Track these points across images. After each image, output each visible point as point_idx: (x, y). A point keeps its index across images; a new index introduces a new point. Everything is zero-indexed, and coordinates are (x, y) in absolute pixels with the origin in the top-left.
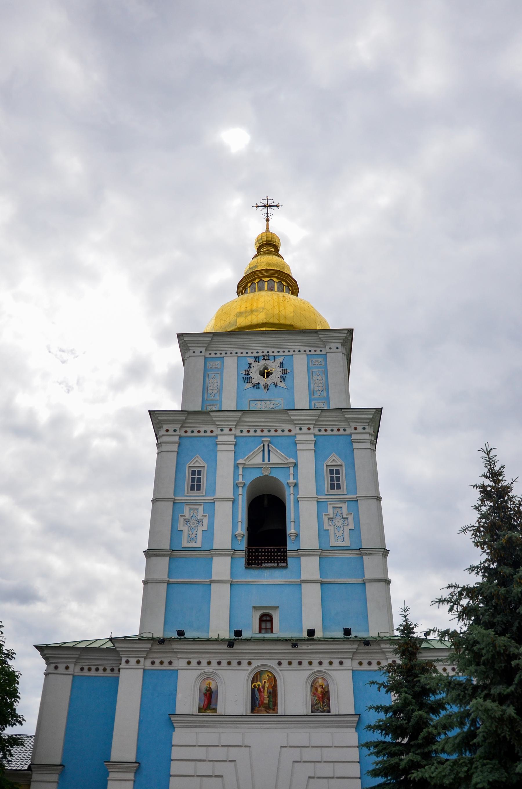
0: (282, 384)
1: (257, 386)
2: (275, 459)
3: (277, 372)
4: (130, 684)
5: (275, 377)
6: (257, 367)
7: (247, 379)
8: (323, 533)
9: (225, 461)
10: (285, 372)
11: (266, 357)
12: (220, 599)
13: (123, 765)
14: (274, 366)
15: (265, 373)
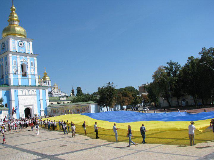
0: (23, 47)
1: (20, 47)
2: (24, 61)
3: (23, 45)
4: (13, 91)
5: (23, 45)
6: (20, 43)
7: (19, 45)
8: (31, 72)
9: (19, 60)
10: (24, 45)
11: (21, 42)
12: (20, 80)
13: (13, 101)
14: (22, 43)
15: (21, 44)
